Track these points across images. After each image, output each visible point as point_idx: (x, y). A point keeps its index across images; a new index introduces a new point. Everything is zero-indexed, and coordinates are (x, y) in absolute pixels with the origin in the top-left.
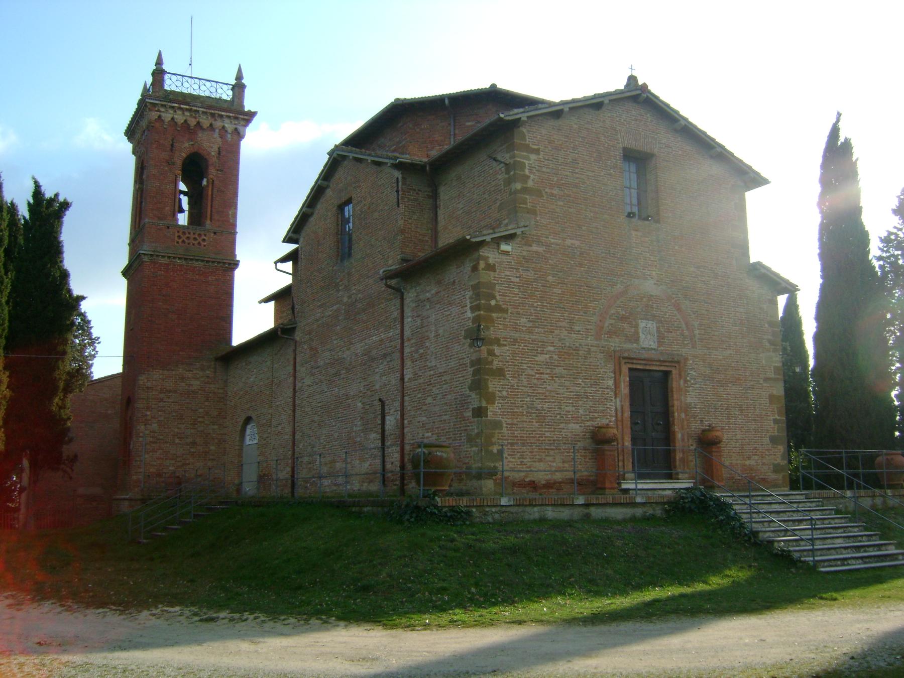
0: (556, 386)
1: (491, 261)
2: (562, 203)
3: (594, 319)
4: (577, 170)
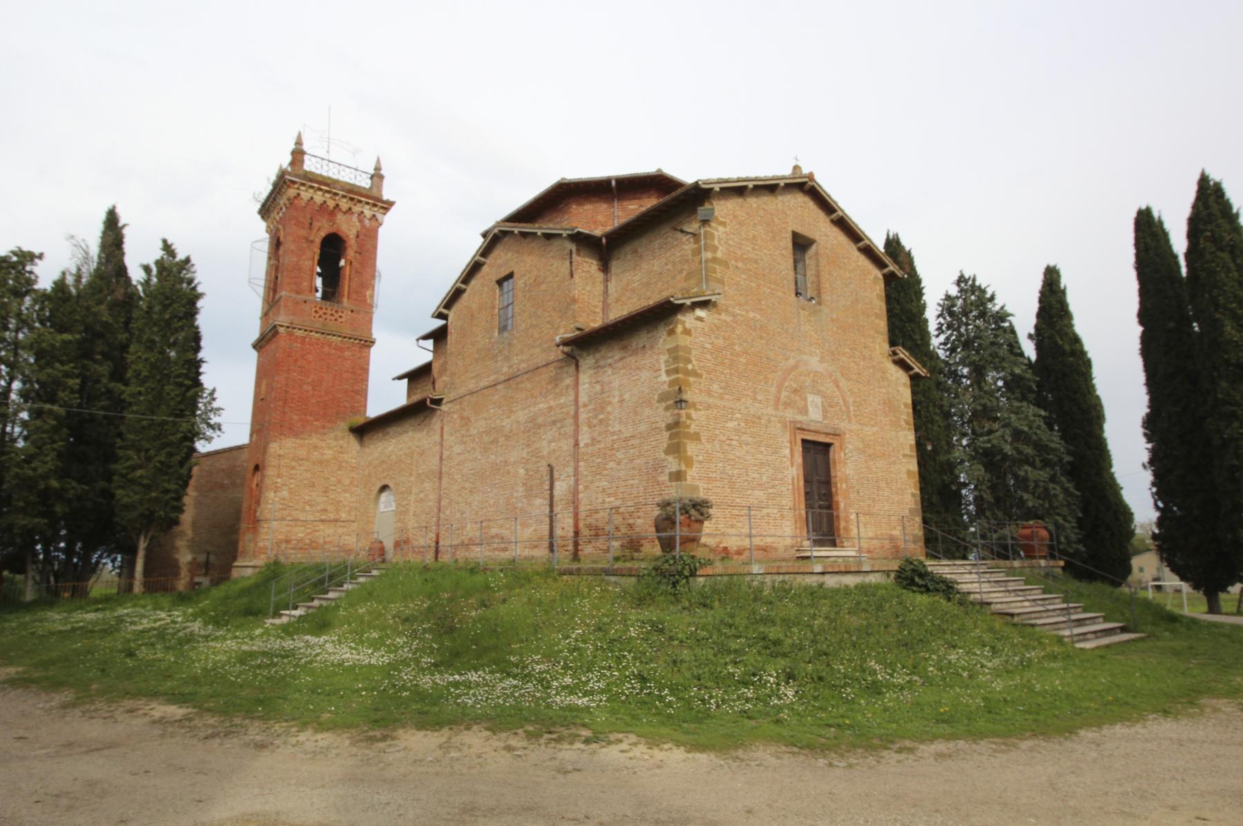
1: (688, 325)
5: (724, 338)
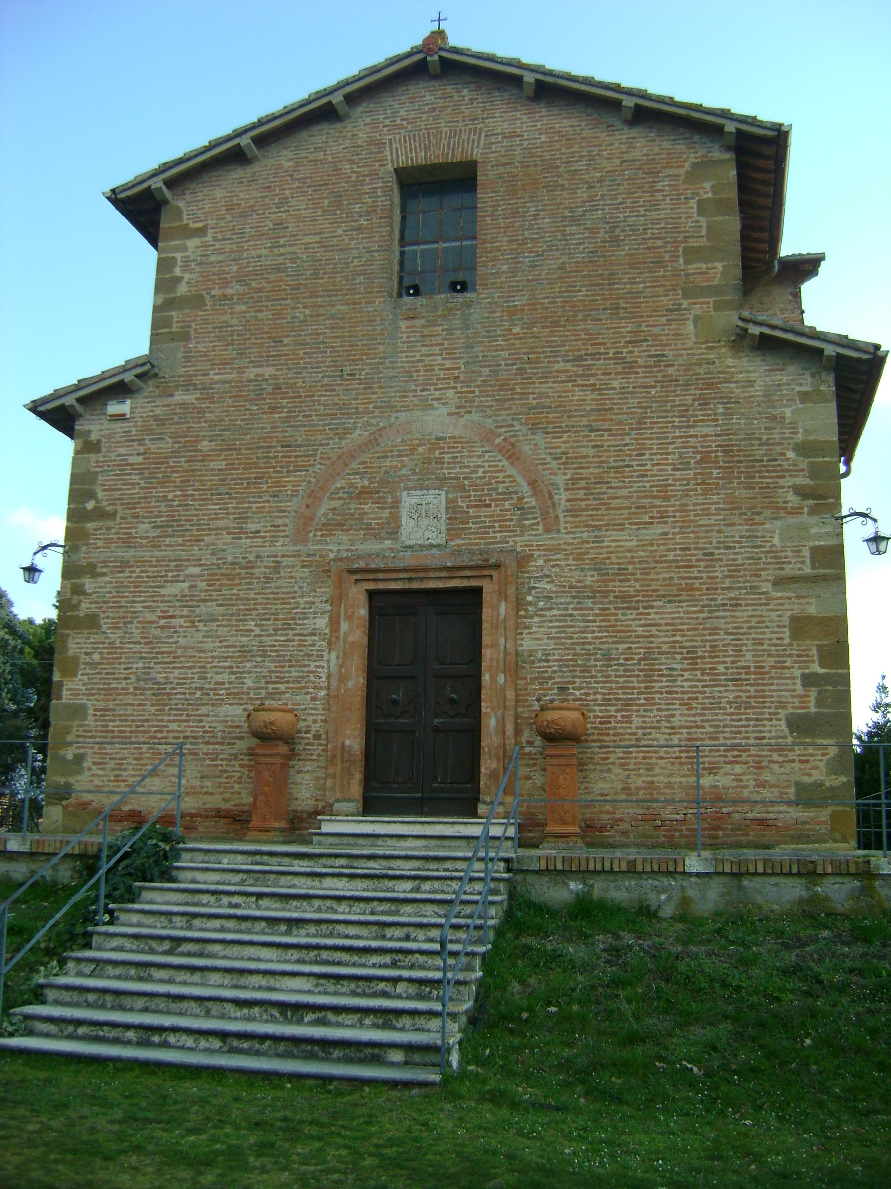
0: (199, 636)
1: (93, 437)
2: (243, 308)
3: (295, 504)
4: (282, 241)
5: (175, 436)
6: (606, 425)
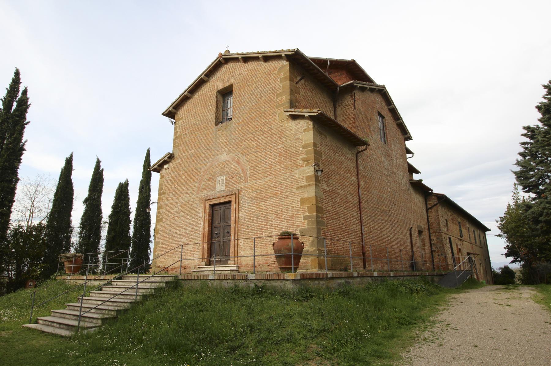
6: (258, 150)
